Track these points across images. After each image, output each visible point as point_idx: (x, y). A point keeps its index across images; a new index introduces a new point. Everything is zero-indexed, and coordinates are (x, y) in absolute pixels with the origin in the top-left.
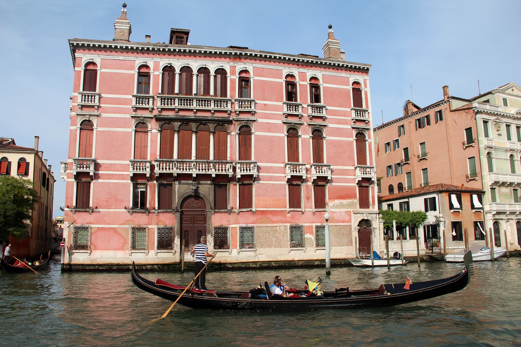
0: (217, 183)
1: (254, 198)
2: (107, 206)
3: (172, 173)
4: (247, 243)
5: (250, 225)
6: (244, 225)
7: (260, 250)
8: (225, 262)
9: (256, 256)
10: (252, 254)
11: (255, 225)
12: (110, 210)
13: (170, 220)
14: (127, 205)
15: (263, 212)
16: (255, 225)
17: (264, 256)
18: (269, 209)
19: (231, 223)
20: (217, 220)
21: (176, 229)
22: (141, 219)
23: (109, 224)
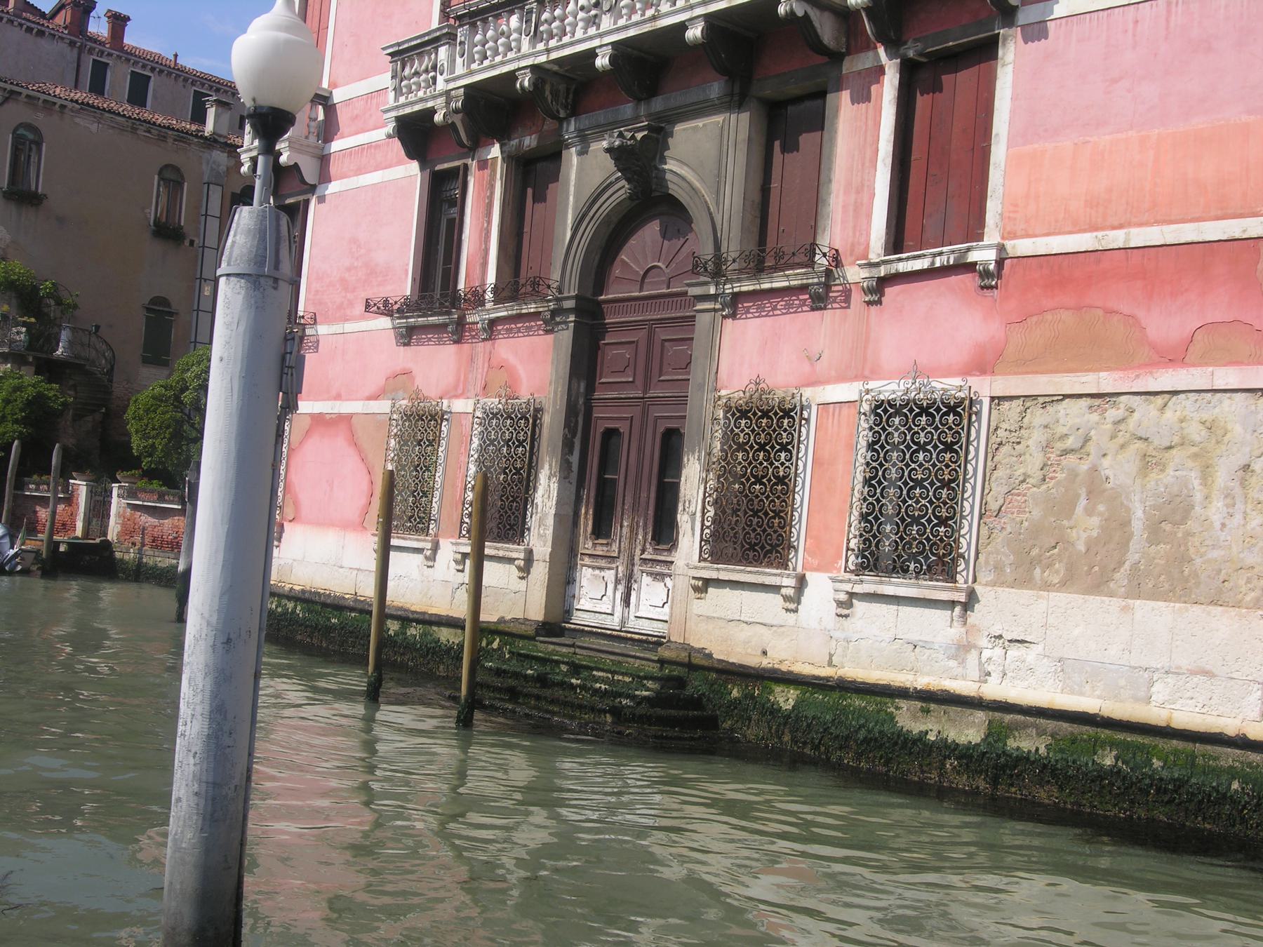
0: (769, 90)
1: (999, 153)
2: (340, 307)
3: (511, 76)
4: (913, 536)
5: (948, 385)
6: (891, 389)
7: (1000, 607)
8: (752, 660)
9: (963, 649)
10: (937, 627)
11: (984, 387)
12: (349, 327)
13: (533, 365)
14: (378, 292)
15: (1060, 272)
16: (984, 387)
17: (1029, 655)
18: (1116, 238)
19: (821, 366)
20: (750, 353)
21: (547, 419)
22: (436, 367)
23: (338, 397)
